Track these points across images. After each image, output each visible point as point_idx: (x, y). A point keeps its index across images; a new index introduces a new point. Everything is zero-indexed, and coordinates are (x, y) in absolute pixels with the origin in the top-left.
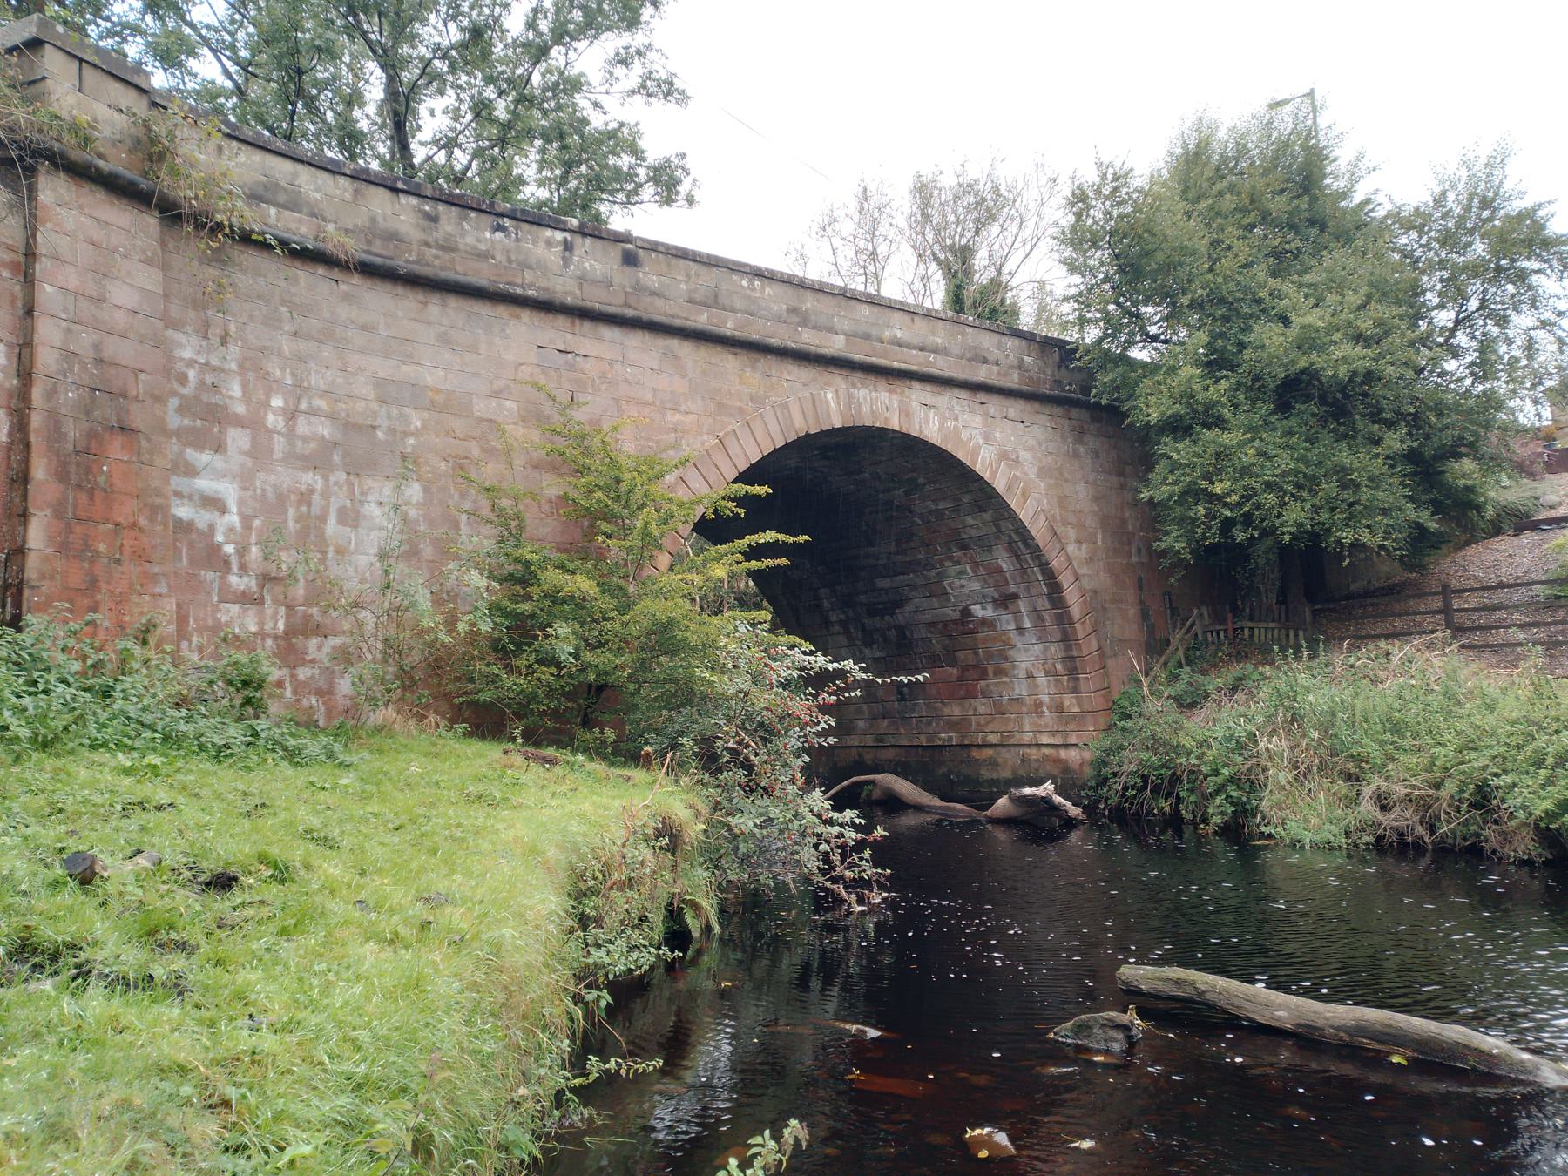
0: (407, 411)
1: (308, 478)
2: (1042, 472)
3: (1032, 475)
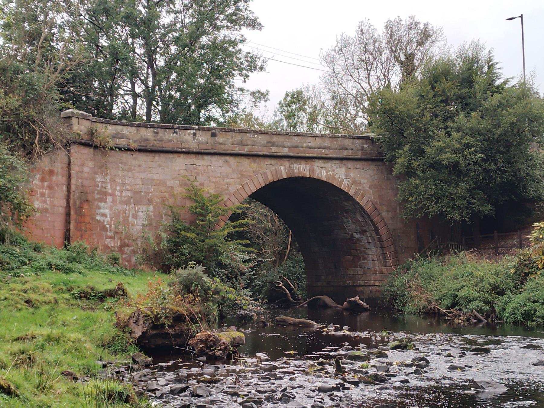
0: (150, 186)
1: (126, 207)
2: (371, 187)
3: (367, 188)
